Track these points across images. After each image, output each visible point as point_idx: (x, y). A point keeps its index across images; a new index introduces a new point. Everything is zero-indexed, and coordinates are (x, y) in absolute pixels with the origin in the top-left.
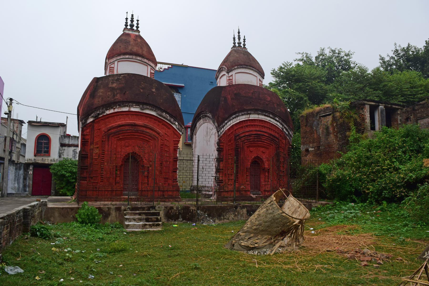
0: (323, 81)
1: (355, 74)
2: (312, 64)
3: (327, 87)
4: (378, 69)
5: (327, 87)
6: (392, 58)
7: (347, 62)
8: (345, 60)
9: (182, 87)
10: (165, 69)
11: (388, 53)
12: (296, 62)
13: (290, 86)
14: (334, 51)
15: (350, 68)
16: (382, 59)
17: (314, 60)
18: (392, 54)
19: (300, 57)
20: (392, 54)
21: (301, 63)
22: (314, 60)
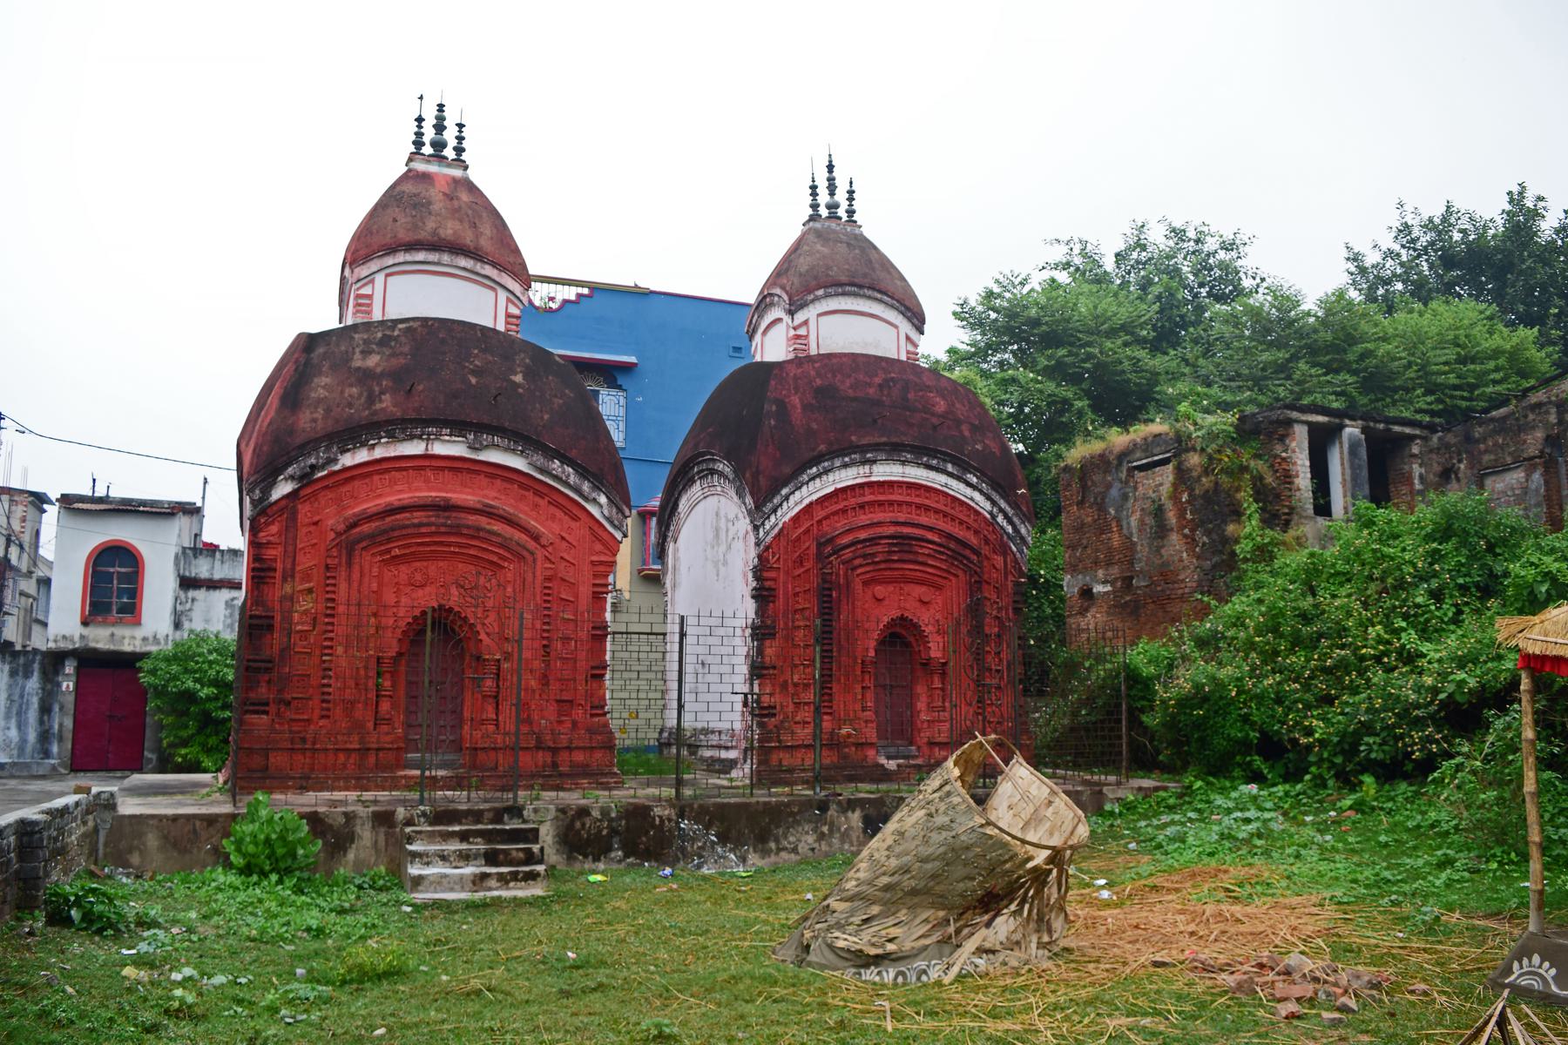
0: (1141, 342)
1: (1256, 314)
2: (1102, 279)
3: (1158, 362)
4: (1340, 294)
5: (1158, 362)
6: (1390, 254)
7: (1230, 273)
8: (1223, 266)
9: (627, 368)
10: (565, 302)
11: (1376, 239)
12: (1046, 274)
13: (1023, 358)
14: (1178, 234)
15: (1239, 292)
16: (1355, 258)
17: (1109, 264)
18: (1388, 242)
19: (1059, 253)
20: (1388, 242)
21: (1063, 277)
22: (1109, 264)
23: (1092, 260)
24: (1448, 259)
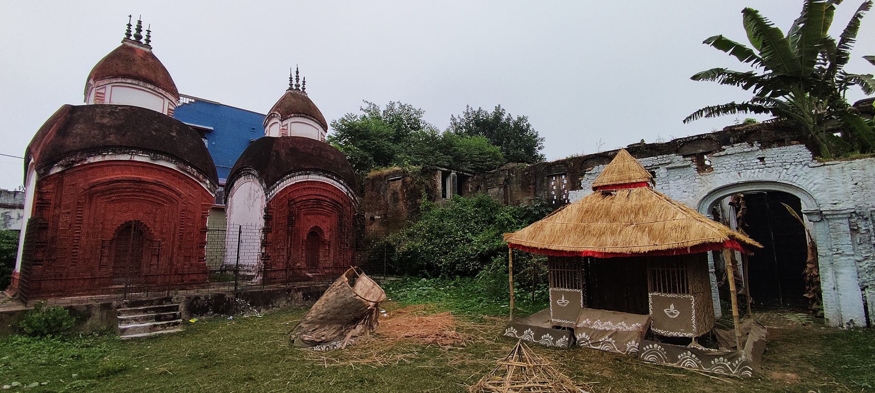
0: (390, 140)
1: (423, 134)
2: (379, 118)
3: (394, 147)
4: (448, 130)
5: (394, 147)
6: (462, 120)
7: (417, 121)
8: (414, 119)
9: (209, 131)
10: (184, 104)
11: (460, 114)
12: (363, 113)
13: (351, 140)
14: (402, 107)
15: (419, 128)
16: (453, 119)
17: (381, 113)
18: (462, 116)
19: (365, 106)
20: (462, 116)
21: (367, 115)
22: (381, 113)
23: (377, 111)
24: (478, 123)
